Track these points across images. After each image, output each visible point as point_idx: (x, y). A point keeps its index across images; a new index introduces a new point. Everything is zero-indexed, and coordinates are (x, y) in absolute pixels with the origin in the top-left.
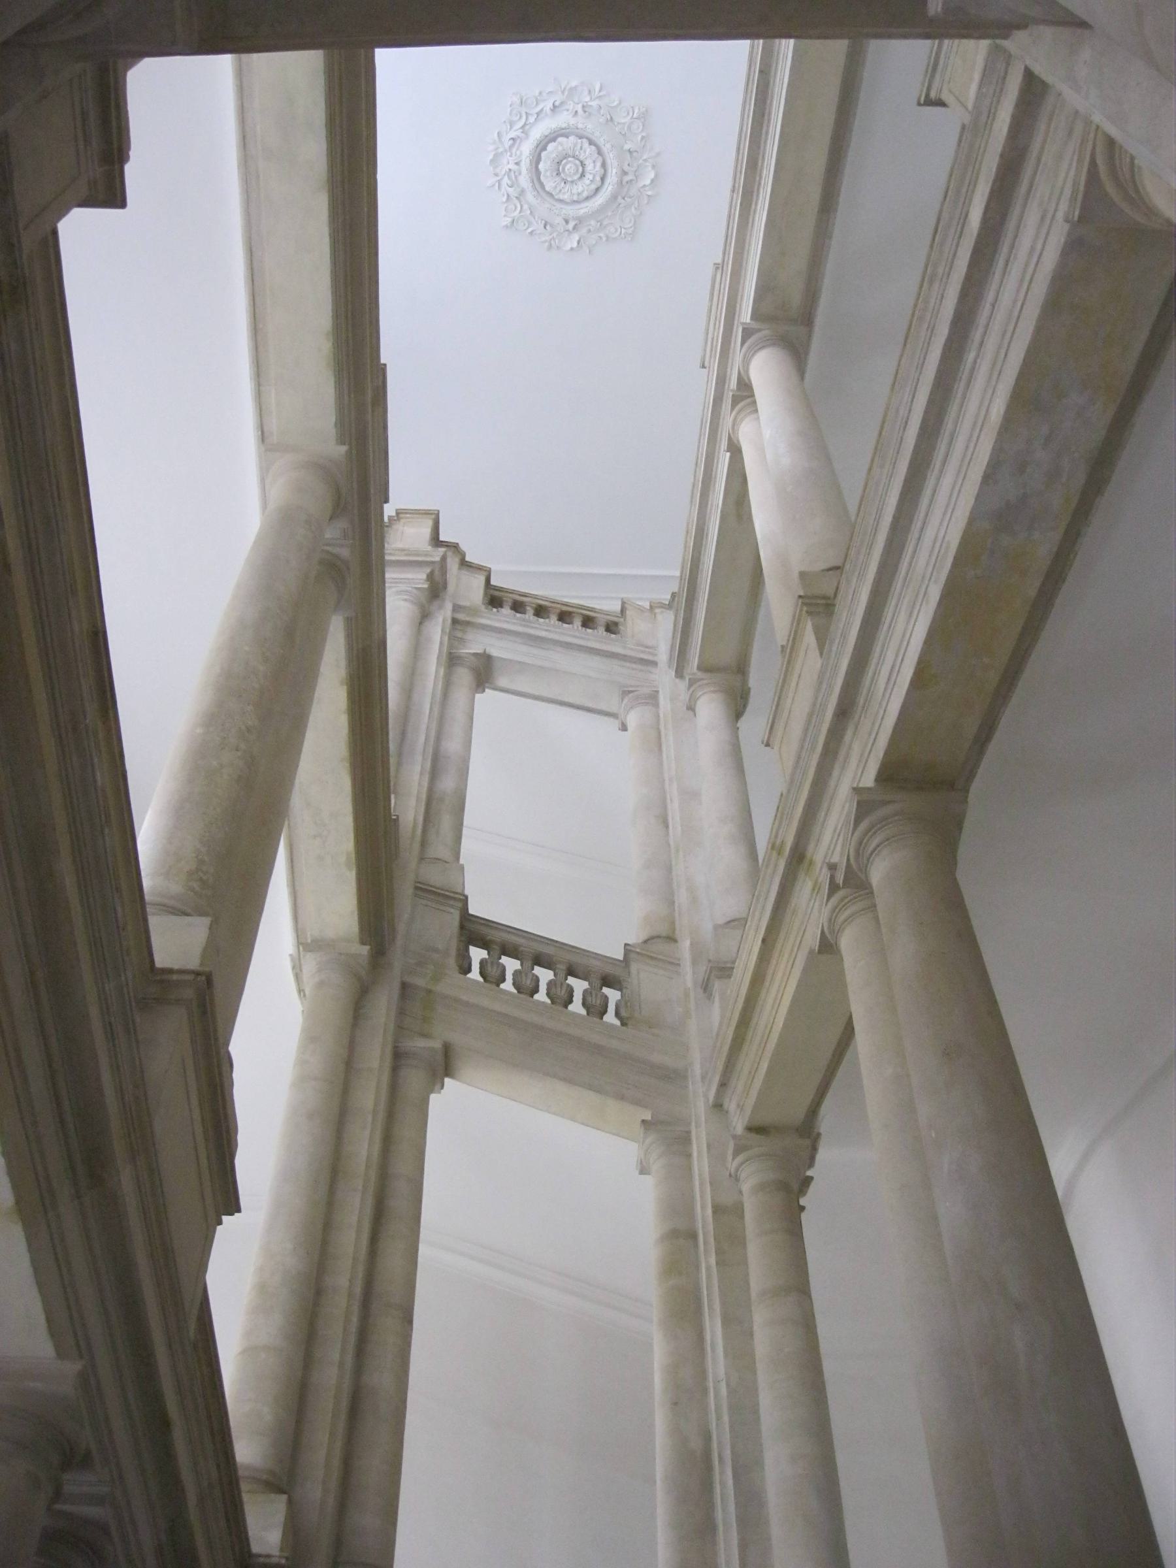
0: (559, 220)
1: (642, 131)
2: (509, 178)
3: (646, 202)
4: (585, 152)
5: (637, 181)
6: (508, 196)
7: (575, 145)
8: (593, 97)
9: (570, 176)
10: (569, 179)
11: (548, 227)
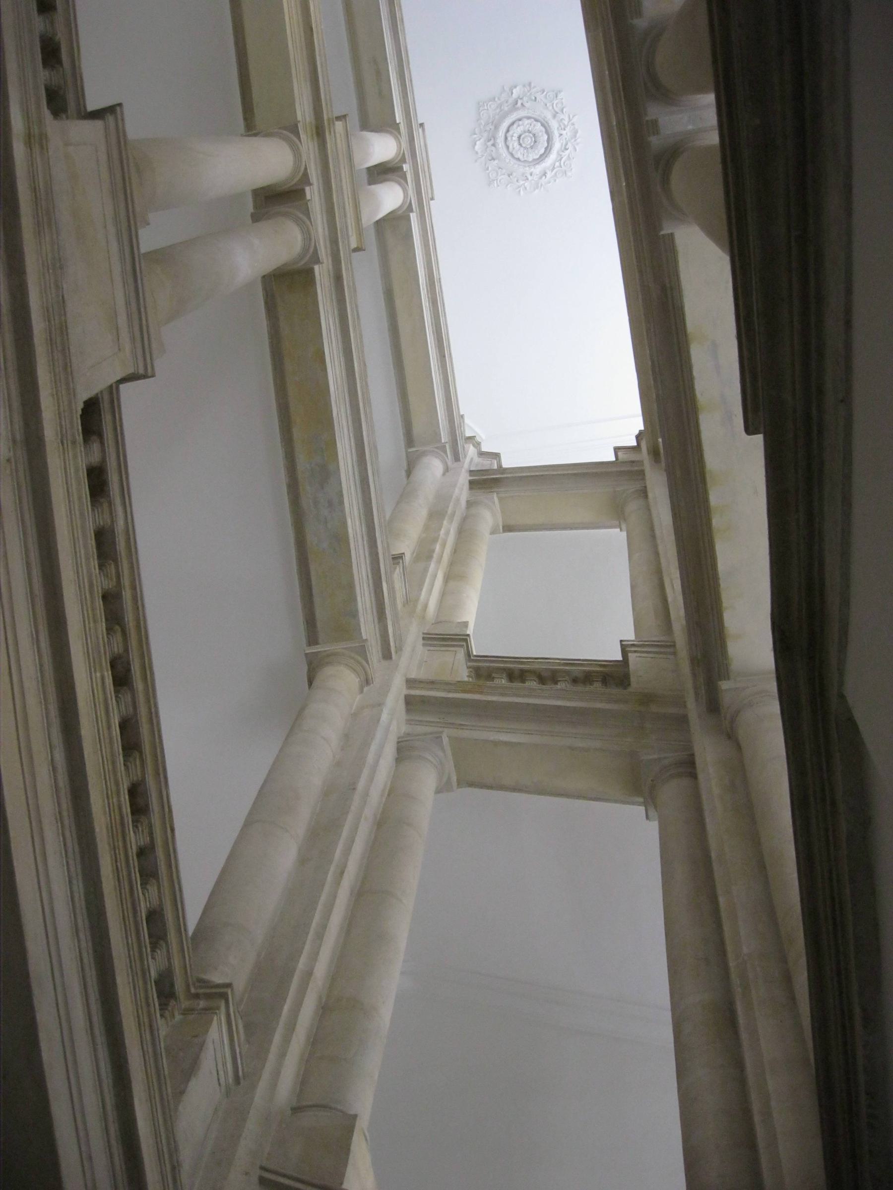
0: (527, 105)
1: (489, 174)
2: (564, 124)
3: (476, 130)
4: (521, 153)
5: (485, 141)
6: (562, 112)
7: (527, 156)
8: (523, 186)
9: (526, 136)
10: (527, 134)
11: (534, 98)
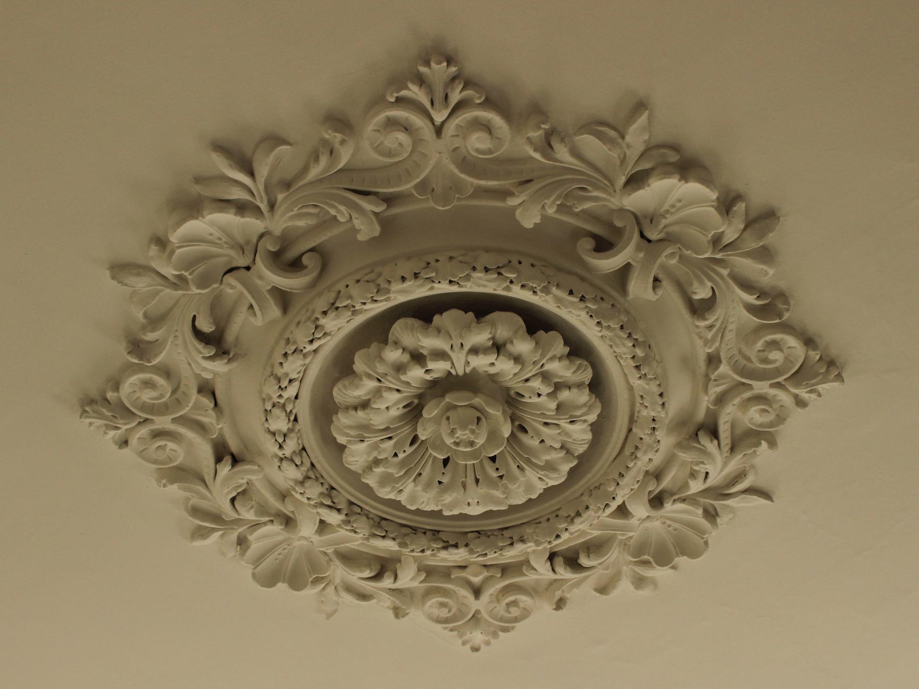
4: (375, 447)
